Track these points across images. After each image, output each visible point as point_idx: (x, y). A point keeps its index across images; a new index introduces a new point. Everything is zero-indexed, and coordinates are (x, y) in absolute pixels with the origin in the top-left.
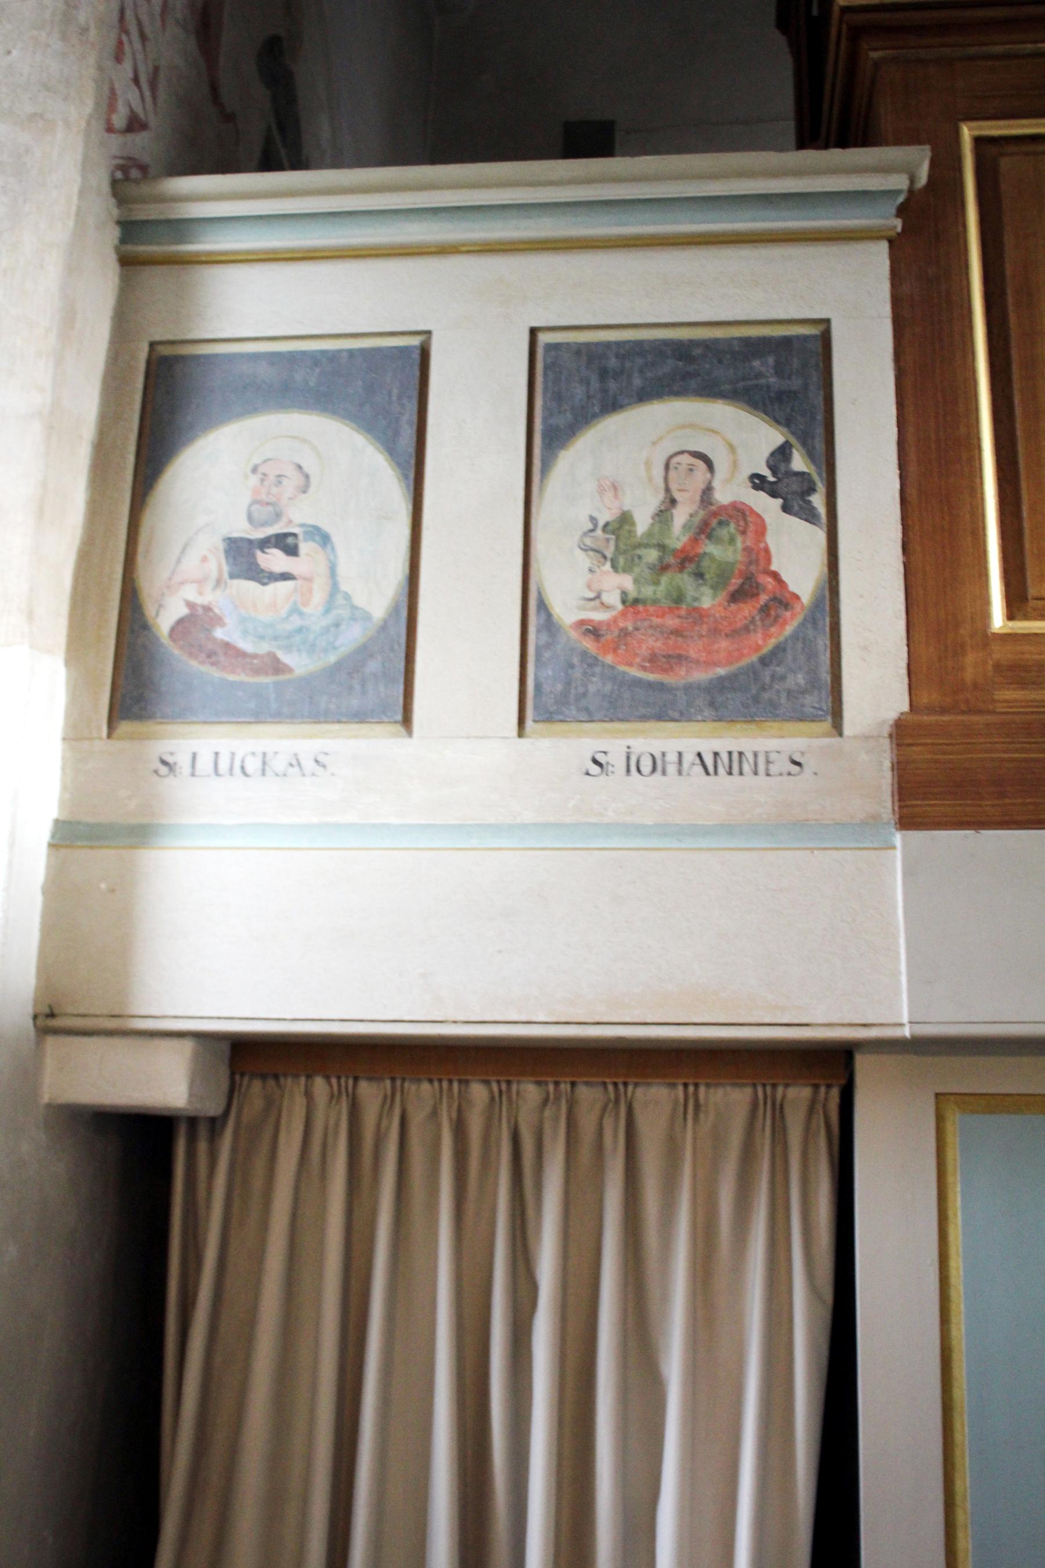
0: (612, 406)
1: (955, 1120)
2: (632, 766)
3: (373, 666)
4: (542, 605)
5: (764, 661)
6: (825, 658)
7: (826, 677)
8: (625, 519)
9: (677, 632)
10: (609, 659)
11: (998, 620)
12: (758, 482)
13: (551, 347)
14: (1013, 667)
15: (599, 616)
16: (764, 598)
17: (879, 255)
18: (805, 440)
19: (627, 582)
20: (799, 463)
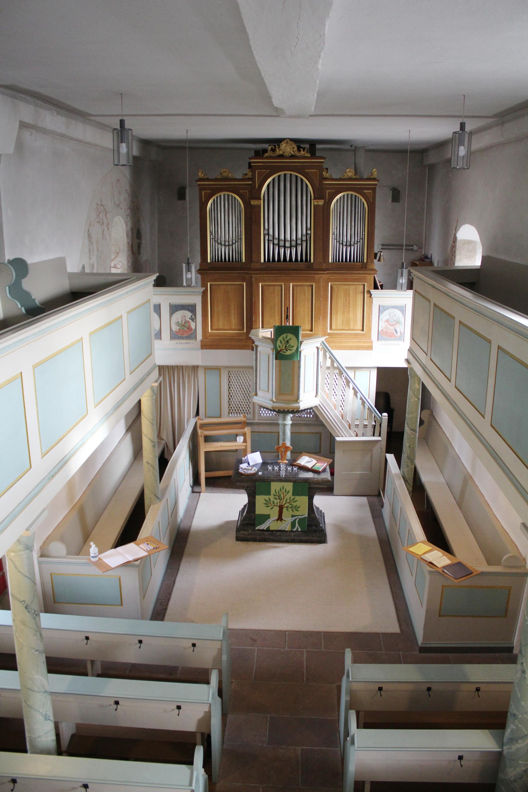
0: (177, 311)
1: (206, 370)
2: (180, 343)
3: (158, 334)
4: (172, 330)
5: (190, 334)
6: (195, 334)
7: (195, 336)
8: (178, 322)
9: (183, 332)
10: (177, 334)
11: (210, 331)
12: (190, 319)
13: (172, 305)
14: (211, 335)
15: (176, 330)
16: (190, 329)
17: (200, 297)
18: (194, 314)
19: (179, 327)
20: (193, 317)
